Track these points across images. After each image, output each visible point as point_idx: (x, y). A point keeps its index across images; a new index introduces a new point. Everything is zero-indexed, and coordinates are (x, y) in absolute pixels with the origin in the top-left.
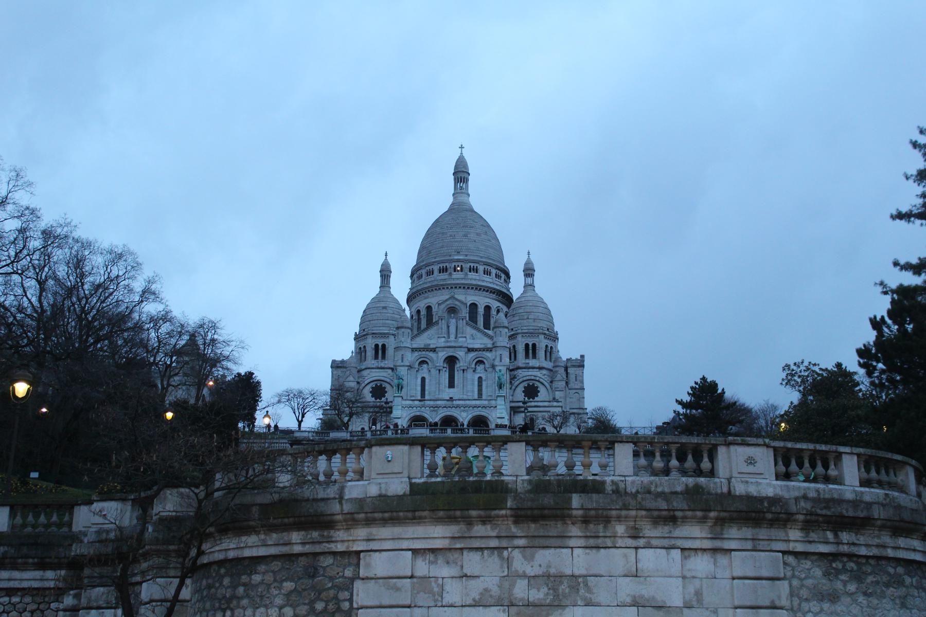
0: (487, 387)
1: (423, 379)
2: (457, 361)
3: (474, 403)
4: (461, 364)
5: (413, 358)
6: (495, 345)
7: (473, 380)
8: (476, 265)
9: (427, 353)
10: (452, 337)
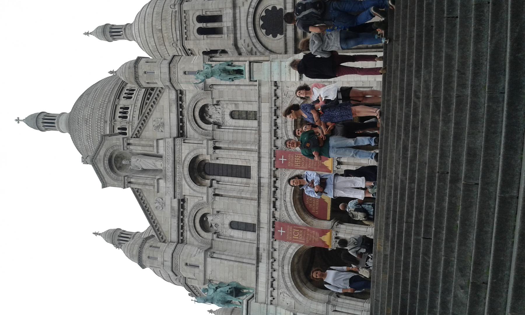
0: (249, 102)
1: (234, 225)
2: (201, 158)
3: (266, 137)
4: (204, 151)
5: (196, 243)
6: (168, 84)
7: (236, 128)
8: (119, 110)
9: (186, 213)
10: (158, 164)
